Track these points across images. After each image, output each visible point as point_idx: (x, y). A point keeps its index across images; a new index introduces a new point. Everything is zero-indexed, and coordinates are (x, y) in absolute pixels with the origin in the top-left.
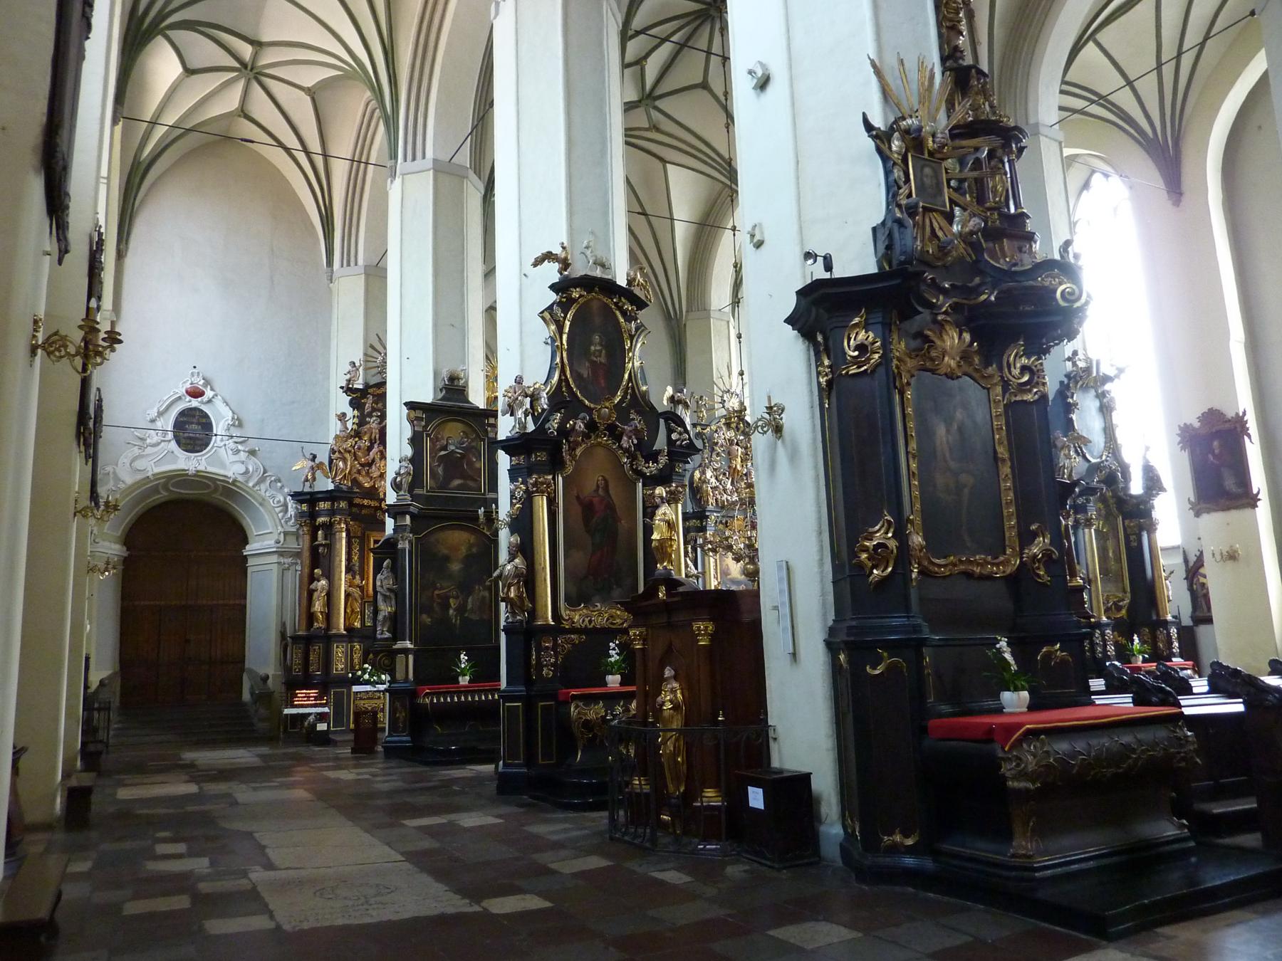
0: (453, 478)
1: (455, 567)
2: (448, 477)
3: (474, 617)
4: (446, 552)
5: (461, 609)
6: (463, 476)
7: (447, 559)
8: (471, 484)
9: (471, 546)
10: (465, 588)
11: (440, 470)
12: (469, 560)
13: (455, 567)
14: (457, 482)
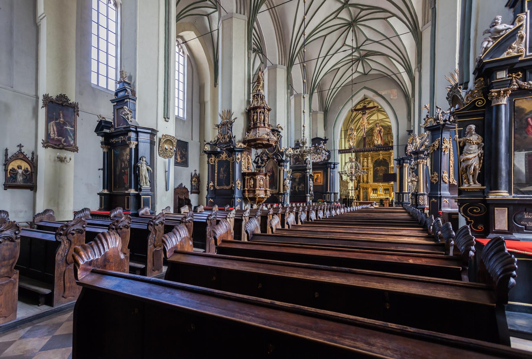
0: (297, 162)
1: (297, 180)
2: (296, 162)
3: (301, 190)
4: (295, 177)
5: (298, 188)
6: (299, 161)
7: (295, 179)
8: (300, 163)
9: (300, 176)
10: (299, 184)
11: (294, 161)
12: (300, 178)
13: (297, 180)
14: (298, 163)
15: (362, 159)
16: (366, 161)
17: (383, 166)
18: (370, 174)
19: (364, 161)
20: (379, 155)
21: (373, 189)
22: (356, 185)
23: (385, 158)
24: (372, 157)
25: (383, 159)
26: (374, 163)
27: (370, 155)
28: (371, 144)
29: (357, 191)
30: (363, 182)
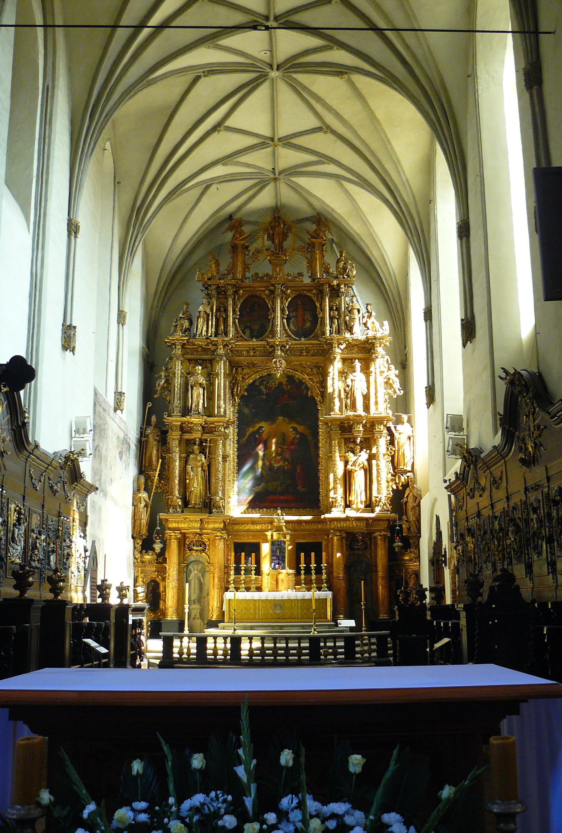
15: (178, 368)
16: (202, 380)
17: (290, 416)
18: (225, 458)
19: (192, 380)
20: (270, 353)
21: (236, 544)
22: (144, 518)
23: (298, 375)
24: (234, 366)
25: (290, 378)
26: (242, 397)
27: (221, 351)
28: (230, 292)
29: (147, 557)
30: (186, 503)
